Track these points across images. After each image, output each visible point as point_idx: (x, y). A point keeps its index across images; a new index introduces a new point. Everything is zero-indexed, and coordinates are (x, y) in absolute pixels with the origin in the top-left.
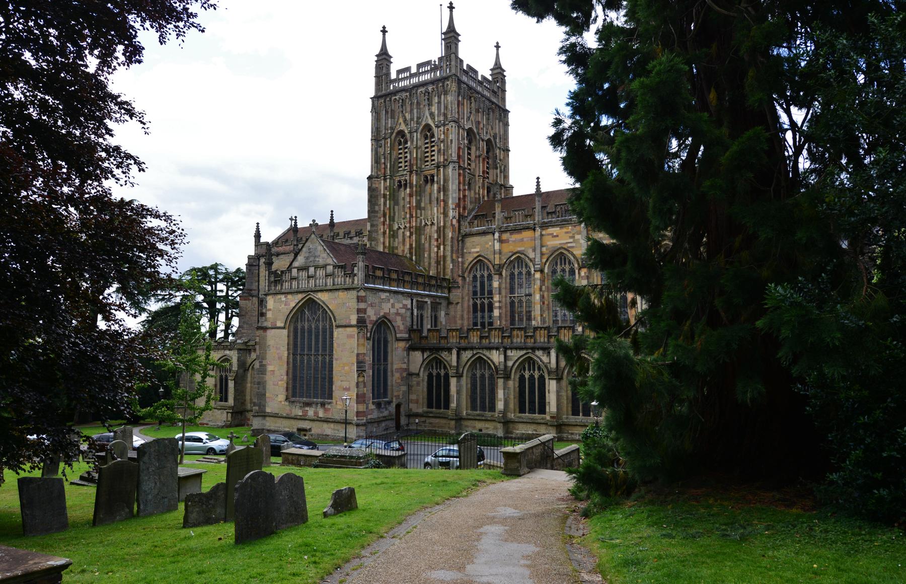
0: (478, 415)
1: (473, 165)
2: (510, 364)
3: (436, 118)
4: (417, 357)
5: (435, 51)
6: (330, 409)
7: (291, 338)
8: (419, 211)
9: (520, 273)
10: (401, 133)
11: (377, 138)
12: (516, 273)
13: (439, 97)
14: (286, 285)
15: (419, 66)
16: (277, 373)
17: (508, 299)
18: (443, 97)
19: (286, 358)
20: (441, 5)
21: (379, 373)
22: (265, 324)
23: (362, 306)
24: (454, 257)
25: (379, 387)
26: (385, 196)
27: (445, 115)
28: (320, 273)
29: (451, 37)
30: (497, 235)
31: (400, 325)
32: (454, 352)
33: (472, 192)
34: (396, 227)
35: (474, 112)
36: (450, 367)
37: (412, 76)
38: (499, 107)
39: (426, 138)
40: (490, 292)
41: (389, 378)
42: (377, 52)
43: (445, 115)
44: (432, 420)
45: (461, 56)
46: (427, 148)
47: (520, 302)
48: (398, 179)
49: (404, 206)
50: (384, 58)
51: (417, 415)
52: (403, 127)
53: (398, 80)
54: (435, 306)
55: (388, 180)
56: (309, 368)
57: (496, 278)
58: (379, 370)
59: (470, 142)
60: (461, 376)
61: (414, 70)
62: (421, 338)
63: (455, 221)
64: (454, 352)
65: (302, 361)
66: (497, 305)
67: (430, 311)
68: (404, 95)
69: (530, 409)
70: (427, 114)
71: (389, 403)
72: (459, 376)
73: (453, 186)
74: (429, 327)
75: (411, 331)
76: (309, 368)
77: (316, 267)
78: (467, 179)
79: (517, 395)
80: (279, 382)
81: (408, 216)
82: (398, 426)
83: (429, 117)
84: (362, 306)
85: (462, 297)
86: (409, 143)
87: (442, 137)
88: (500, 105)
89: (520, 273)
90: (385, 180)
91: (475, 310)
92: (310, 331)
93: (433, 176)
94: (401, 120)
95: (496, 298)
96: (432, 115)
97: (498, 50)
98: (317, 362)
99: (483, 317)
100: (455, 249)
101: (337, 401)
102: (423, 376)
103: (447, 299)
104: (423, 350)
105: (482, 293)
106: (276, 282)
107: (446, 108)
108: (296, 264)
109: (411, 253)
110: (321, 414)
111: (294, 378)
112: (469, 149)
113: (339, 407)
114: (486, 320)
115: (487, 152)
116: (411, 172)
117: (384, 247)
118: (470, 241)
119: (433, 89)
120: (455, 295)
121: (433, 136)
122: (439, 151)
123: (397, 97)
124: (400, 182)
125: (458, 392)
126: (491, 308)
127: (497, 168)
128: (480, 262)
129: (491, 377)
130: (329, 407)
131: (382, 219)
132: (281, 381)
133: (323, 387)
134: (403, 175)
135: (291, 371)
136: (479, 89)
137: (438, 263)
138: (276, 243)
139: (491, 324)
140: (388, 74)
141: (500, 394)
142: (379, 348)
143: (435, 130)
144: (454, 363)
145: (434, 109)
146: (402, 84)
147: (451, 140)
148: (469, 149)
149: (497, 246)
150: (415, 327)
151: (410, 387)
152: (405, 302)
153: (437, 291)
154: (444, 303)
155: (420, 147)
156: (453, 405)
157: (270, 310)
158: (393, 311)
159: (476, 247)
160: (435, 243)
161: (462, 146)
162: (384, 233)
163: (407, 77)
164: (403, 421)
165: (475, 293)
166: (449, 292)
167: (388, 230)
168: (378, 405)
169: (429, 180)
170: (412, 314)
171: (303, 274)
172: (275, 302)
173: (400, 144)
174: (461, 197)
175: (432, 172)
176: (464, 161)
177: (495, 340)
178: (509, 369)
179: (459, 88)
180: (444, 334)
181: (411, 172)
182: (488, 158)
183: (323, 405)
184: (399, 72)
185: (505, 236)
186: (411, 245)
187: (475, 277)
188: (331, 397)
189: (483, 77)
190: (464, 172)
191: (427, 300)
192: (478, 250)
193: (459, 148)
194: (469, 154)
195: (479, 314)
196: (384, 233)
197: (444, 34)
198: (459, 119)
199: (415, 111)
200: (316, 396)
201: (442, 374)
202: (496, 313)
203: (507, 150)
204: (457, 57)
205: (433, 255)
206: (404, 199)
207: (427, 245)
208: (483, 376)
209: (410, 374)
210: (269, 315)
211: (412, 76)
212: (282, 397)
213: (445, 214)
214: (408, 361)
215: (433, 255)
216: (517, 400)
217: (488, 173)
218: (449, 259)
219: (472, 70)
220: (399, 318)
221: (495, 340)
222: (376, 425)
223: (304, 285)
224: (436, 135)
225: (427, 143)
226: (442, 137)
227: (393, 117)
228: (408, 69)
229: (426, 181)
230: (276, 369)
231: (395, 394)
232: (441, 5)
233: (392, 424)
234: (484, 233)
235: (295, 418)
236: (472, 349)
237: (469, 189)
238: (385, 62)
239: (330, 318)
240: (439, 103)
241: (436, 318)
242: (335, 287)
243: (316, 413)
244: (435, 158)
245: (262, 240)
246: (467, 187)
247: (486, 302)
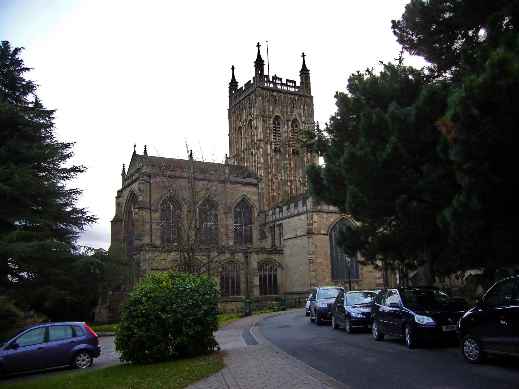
3: (303, 118)
6: (361, 284)
10: (277, 118)
15: (288, 81)
18: (306, 106)
19: (330, 254)
20: (267, 41)
52: (280, 115)
65: (337, 256)
68: (279, 94)
80: (326, 270)
83: (297, 115)
101: (365, 279)
113: (367, 282)
119: (298, 99)
123: (275, 94)
124: (275, 148)
130: (361, 283)
132: (327, 269)
134: (278, 145)
157: (315, 222)
172: (318, 217)
175: (298, 149)
188: (357, 277)
200: (342, 279)
211: (282, 84)
230: (323, 261)
232: (267, 41)
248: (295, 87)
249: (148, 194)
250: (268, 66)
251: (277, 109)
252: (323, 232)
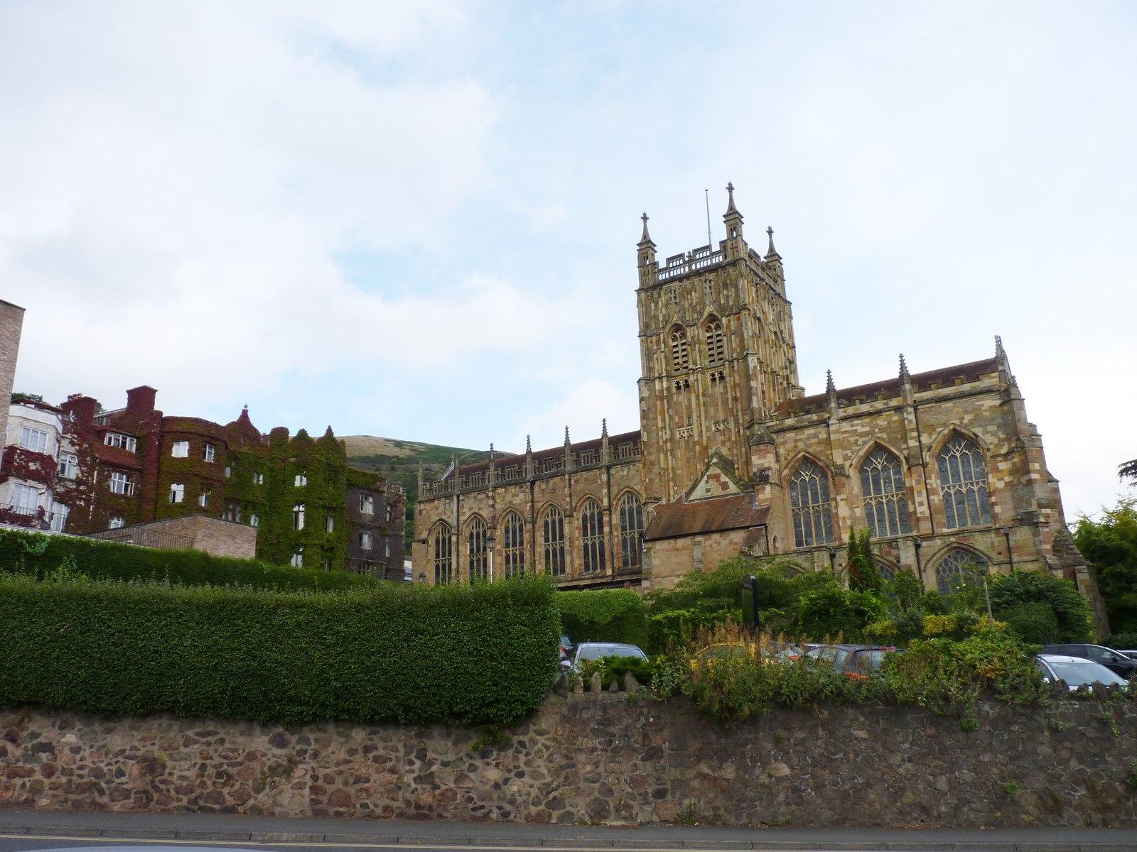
11: (646, 333)
29: (733, 219)
42: (639, 240)
45: (745, 238)
53: (667, 269)
97: (770, 236)
140: (655, 264)
146: (673, 273)
163: (680, 265)
184: (669, 260)
204: (743, 240)
219: (753, 255)
238: (651, 251)
248: (714, 254)
250: (709, 232)
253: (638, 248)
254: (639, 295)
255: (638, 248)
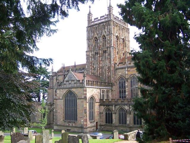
0: (121, 125)
1: (118, 46)
2: (131, 109)
4: (103, 107)
5: (106, 12)
7: (64, 102)
8: (102, 62)
9: (134, 81)
10: (96, 38)
11: (89, 39)
12: (133, 81)
13: (107, 26)
14: (63, 86)
15: (101, 17)
16: (60, 113)
17: (130, 89)
21: (91, 113)
22: (56, 98)
23: (85, 93)
24: (113, 76)
25: (91, 117)
26: (91, 57)
27: (109, 32)
28: (73, 82)
30: (126, 69)
31: (97, 98)
32: (114, 106)
33: (118, 55)
34: (95, 67)
35: (118, 30)
36: (113, 111)
37: (99, 20)
38: (126, 28)
39: (104, 39)
40: (125, 87)
41: (94, 114)
42: (88, 14)
43: (109, 32)
44: (107, 127)
46: (104, 42)
47: (134, 90)
48: (95, 52)
49: (97, 60)
50: (90, 14)
51: (102, 125)
52: (96, 36)
54: (108, 92)
55: (92, 52)
56: (70, 111)
57: (126, 82)
58: (91, 113)
59: (117, 40)
60: (116, 113)
61: (99, 18)
62: (103, 102)
63: (113, 65)
64: (114, 106)
65: (68, 109)
66: (127, 91)
67: (106, 93)
68: (96, 26)
69: (137, 123)
70: (104, 31)
71: (94, 122)
72: (116, 113)
73: (112, 54)
74: (106, 98)
75: (100, 100)
76: (70, 111)
77: (71, 81)
78: (117, 51)
79: (133, 119)
81: (99, 63)
82: (97, 129)
84: (85, 93)
85: (116, 88)
86: (98, 41)
87: (109, 39)
88: (126, 27)
89: (134, 81)
90: (91, 52)
91: (120, 93)
92: (70, 100)
93: (106, 51)
94: (96, 34)
95: (127, 89)
96: (105, 32)
98: (72, 109)
99: (123, 95)
100: (113, 73)
102: (104, 113)
103: (111, 89)
104: (104, 106)
105: (122, 87)
106: (60, 85)
107: (110, 30)
108: (65, 80)
109: (100, 75)
110: (74, 125)
111: (66, 114)
112: (117, 42)
114: (124, 96)
115: (123, 42)
116: (99, 50)
117: (92, 73)
118: (118, 71)
120: (114, 88)
121: (106, 38)
122: (108, 43)
125: (115, 118)
126: (125, 92)
127: (126, 47)
128: (121, 77)
129: (125, 114)
130: (76, 123)
131: (91, 64)
133: (74, 117)
135: (64, 112)
136: (119, 23)
137: (108, 78)
138: (58, 72)
139: (125, 97)
140: (91, 20)
141: (128, 119)
142: (91, 105)
143: (106, 37)
144: (114, 110)
145: (106, 30)
146: (96, 23)
147: (111, 40)
148: (117, 42)
149: (127, 72)
150: (101, 98)
151: (100, 117)
152: (98, 91)
153: (108, 87)
154: (110, 90)
155: (102, 42)
156: (114, 122)
157: (58, 94)
158: (95, 94)
159: (120, 73)
160: (107, 72)
161: (115, 41)
162: (91, 69)
164: (99, 127)
165: (120, 87)
166: (112, 86)
167: (92, 68)
168: (91, 122)
169: (105, 52)
170: (100, 94)
171: (68, 83)
173: (95, 41)
174: (115, 57)
175: (106, 49)
176: (115, 46)
177: (126, 102)
178: (130, 111)
179: (113, 23)
180: (110, 100)
181: (99, 50)
182: (123, 44)
183: (74, 122)
184: (95, 19)
185: (129, 69)
186: (100, 72)
187: (120, 82)
188: (77, 120)
189: (121, 19)
190: (116, 49)
191: (105, 90)
192: (121, 74)
193: (114, 42)
194: (117, 43)
195: (121, 94)
196: (91, 69)
197: (108, 7)
198: (113, 33)
199: (100, 31)
200: (72, 120)
201: (110, 113)
202: (127, 93)
203: (129, 41)
204: (112, 14)
205: (107, 75)
206: (97, 58)
207: (105, 72)
208: (122, 113)
209: (100, 113)
210: (58, 95)
211: (99, 20)
212: (62, 120)
213: (110, 62)
214: (100, 109)
215: (107, 75)
216: (133, 121)
217: (123, 49)
218: (112, 77)
220: (96, 96)
221: (126, 102)
222: (90, 128)
223: (68, 86)
224: (107, 38)
225: (104, 41)
226: (109, 39)
227: (93, 33)
228: (97, 18)
229: (104, 52)
231: (96, 119)
233: (95, 128)
234: (122, 68)
235: (66, 126)
236: (119, 105)
237: (118, 54)
238: (91, 16)
239: (76, 96)
240: (107, 28)
241: (108, 95)
242: (77, 87)
243: (72, 125)
244: (106, 45)
245: (54, 71)
246: (117, 54)
247: (124, 90)
249: (52, 83)
251: (96, 34)
252: (61, 98)
253: (88, 15)
254: (87, 29)
255: (88, 15)
